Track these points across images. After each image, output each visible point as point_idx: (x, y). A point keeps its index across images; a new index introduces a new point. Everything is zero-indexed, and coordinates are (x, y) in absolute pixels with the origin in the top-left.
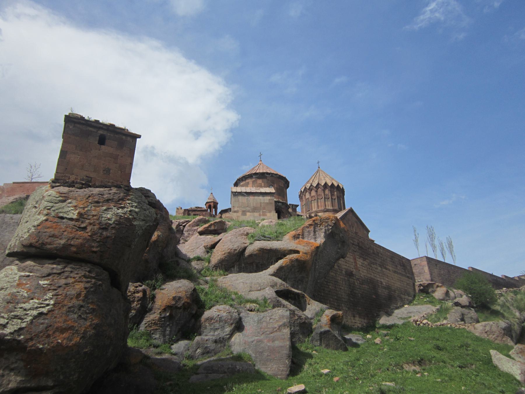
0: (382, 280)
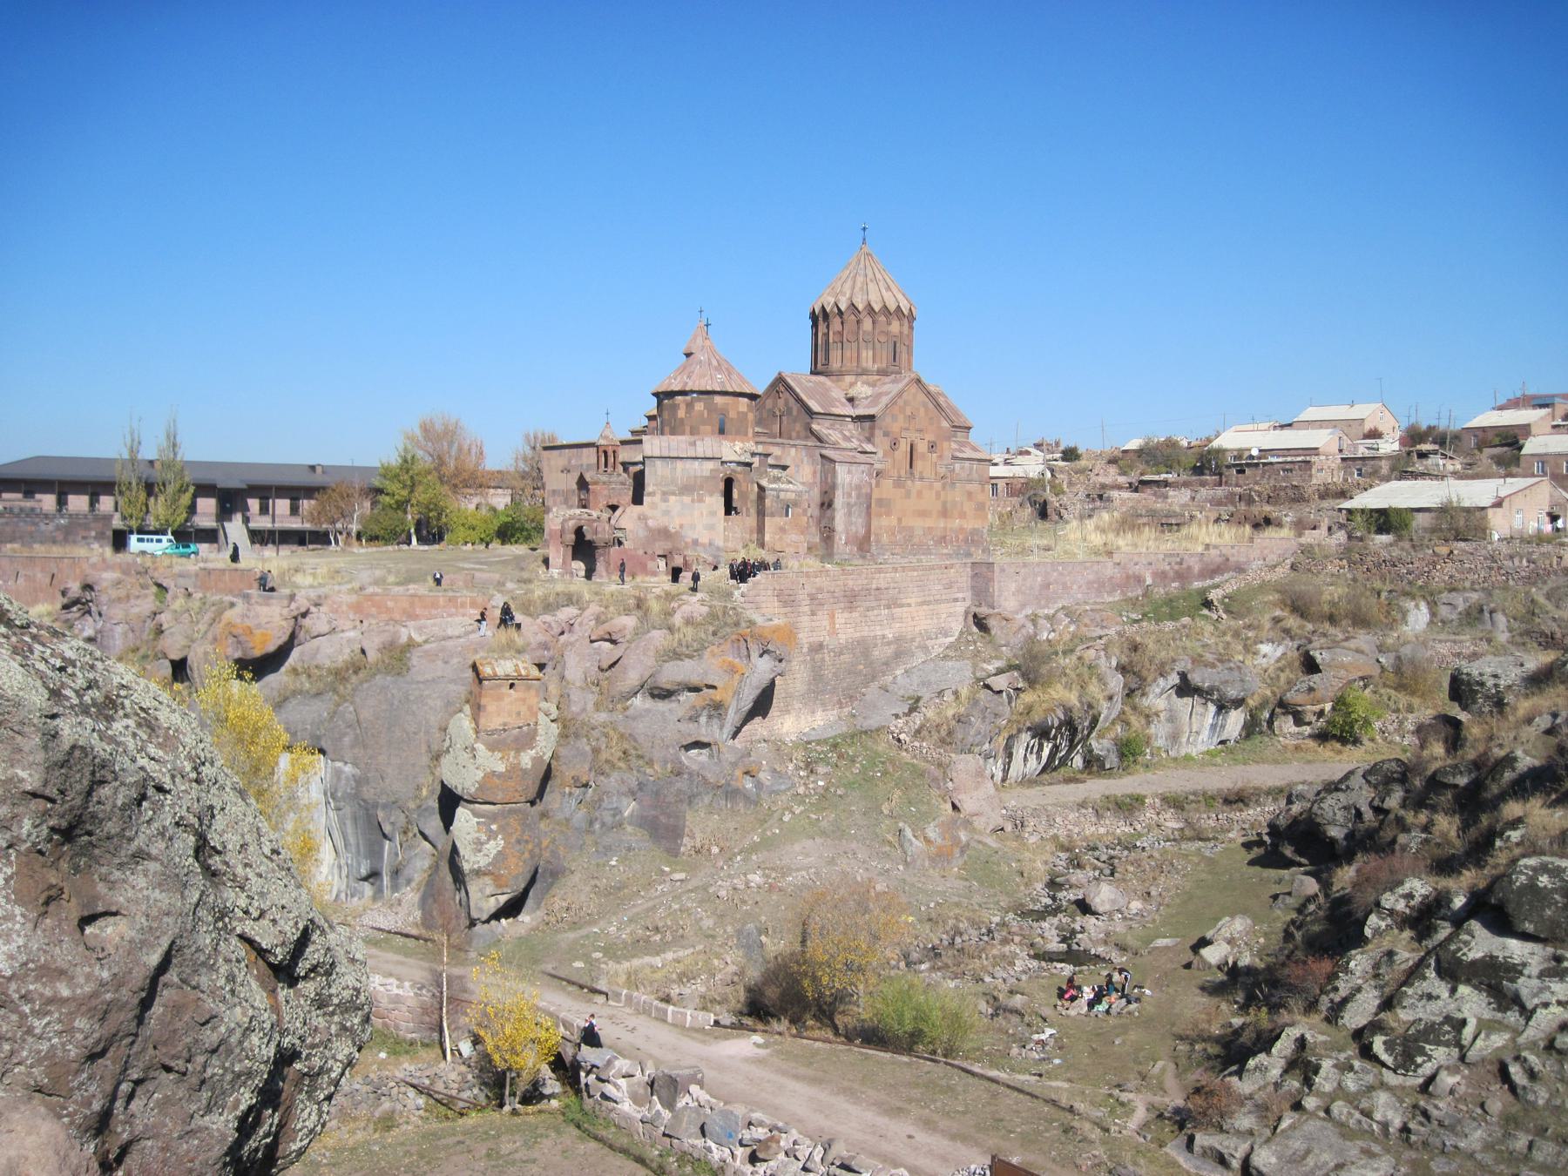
0: (886, 632)
